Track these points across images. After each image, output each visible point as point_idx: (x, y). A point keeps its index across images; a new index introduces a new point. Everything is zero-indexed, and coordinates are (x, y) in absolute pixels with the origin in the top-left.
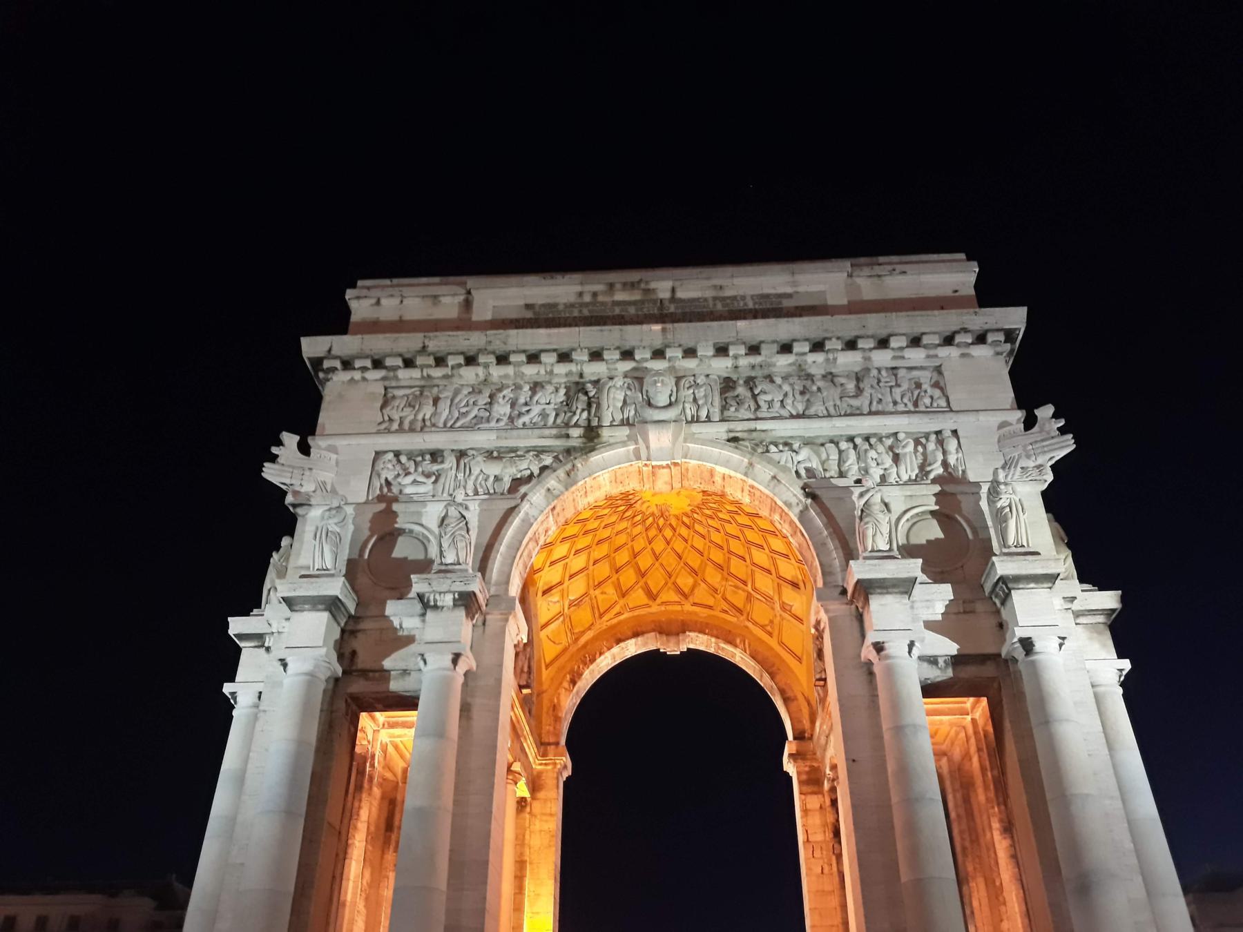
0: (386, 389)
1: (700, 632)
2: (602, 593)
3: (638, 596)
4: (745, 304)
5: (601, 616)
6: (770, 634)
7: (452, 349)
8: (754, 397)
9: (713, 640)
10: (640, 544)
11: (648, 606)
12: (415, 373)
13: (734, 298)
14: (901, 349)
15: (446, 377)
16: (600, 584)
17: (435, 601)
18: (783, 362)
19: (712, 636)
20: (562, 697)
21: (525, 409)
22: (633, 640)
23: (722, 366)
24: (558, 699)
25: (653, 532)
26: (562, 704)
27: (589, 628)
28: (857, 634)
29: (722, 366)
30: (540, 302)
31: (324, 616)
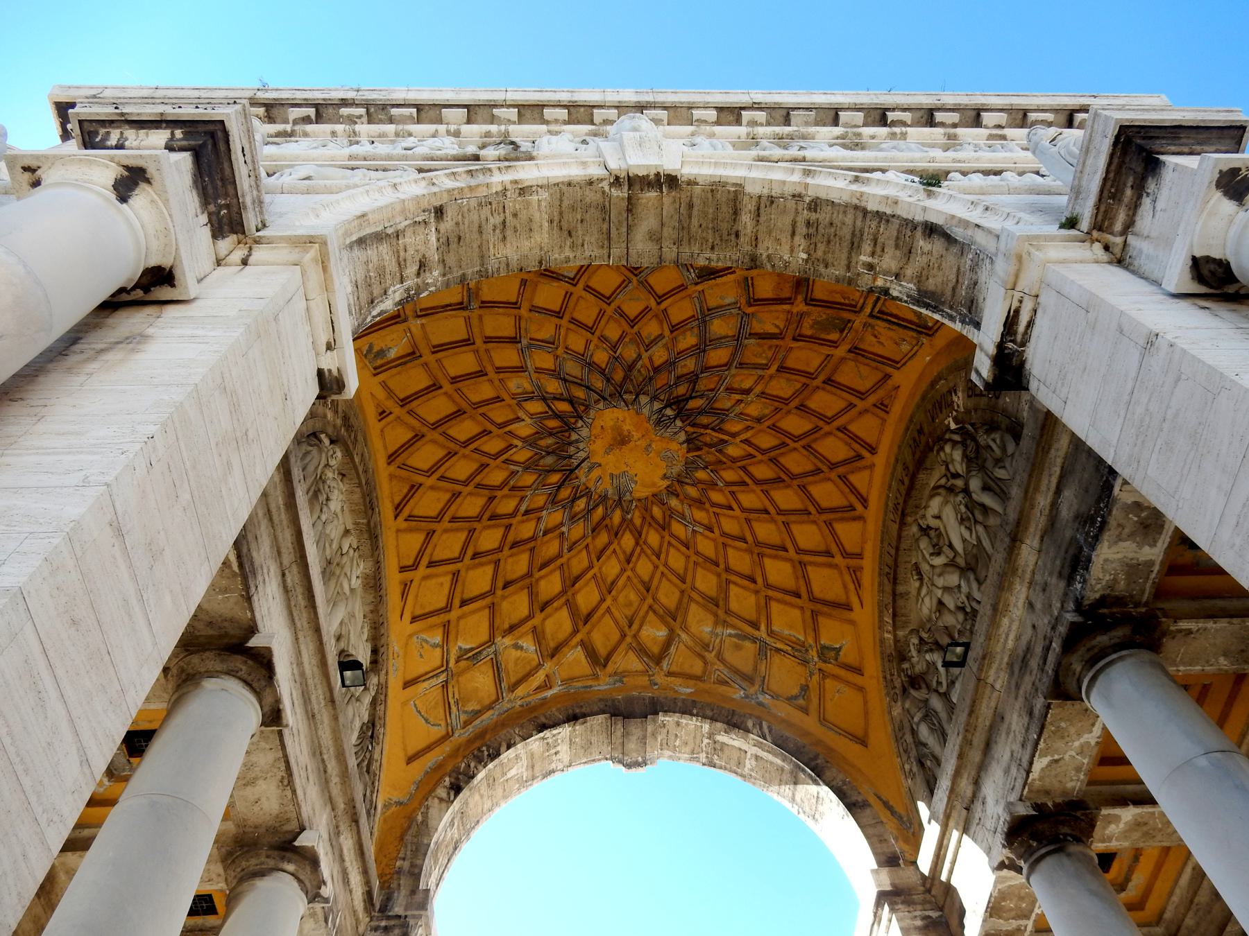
1: (683, 712)
2: (517, 647)
3: (575, 657)
5: (513, 687)
6: (805, 710)
9: (706, 727)
10: (579, 561)
11: (595, 677)
16: (512, 628)
19: (704, 717)
20: (433, 812)
22: (564, 731)
24: (425, 815)
25: (603, 538)
26: (431, 823)
27: (490, 707)
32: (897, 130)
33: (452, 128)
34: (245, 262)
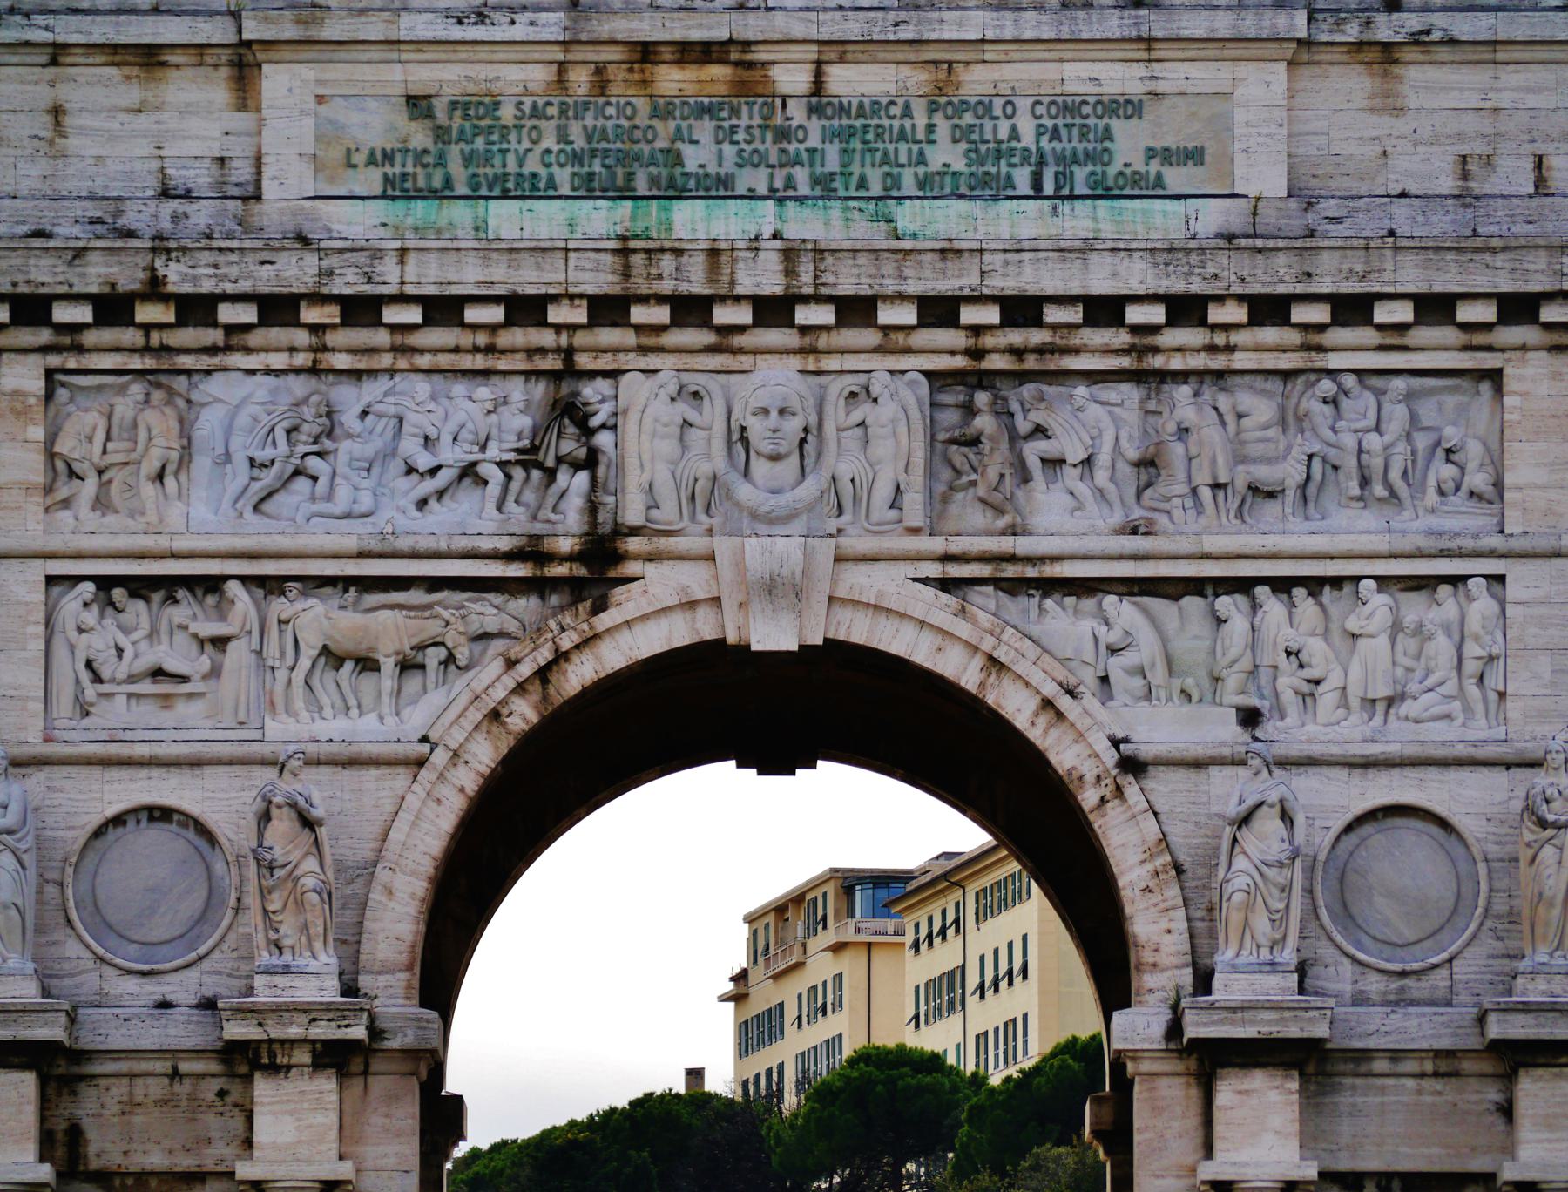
0: (50, 373)
4: (1014, 135)
7: (229, 288)
8: (1014, 437)
12: (131, 336)
13: (984, 108)
14: (1401, 328)
15: (212, 350)
17: (272, 1055)
18: (1099, 347)
21: (424, 461)
23: (942, 348)
28: (1193, 1121)
29: (942, 348)
30: (450, 92)
31: (27, 1082)
32: (1220, 339)
33: (482, 339)
34: (365, 1073)
